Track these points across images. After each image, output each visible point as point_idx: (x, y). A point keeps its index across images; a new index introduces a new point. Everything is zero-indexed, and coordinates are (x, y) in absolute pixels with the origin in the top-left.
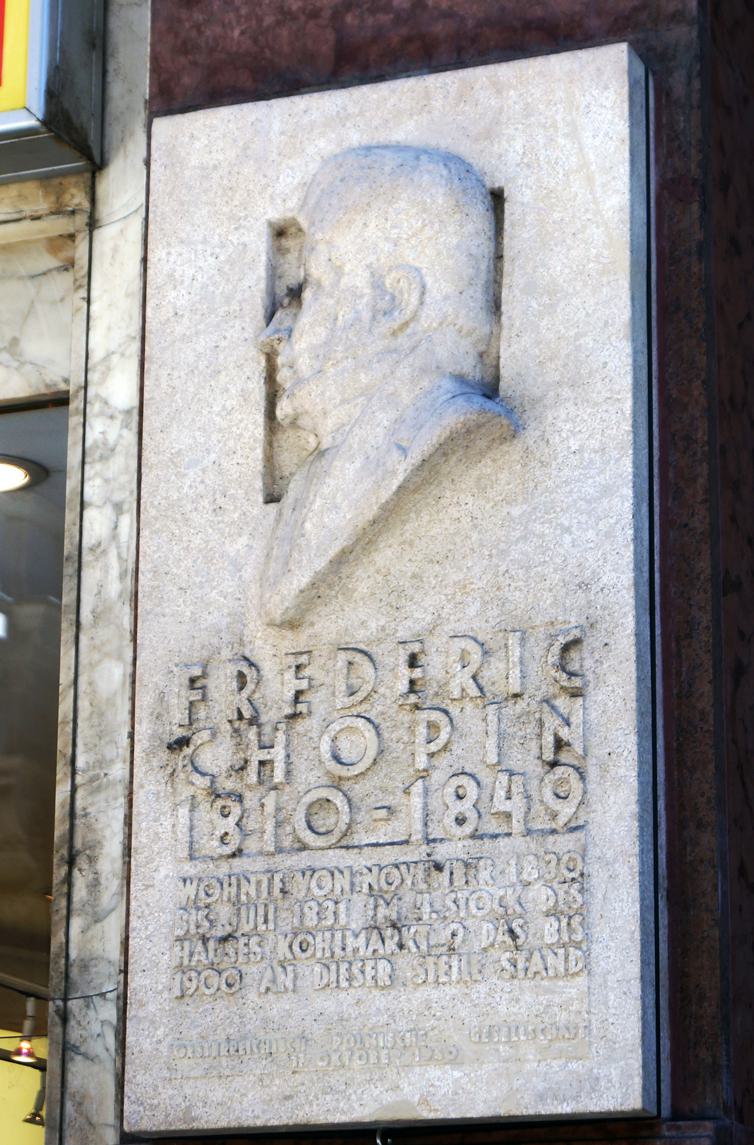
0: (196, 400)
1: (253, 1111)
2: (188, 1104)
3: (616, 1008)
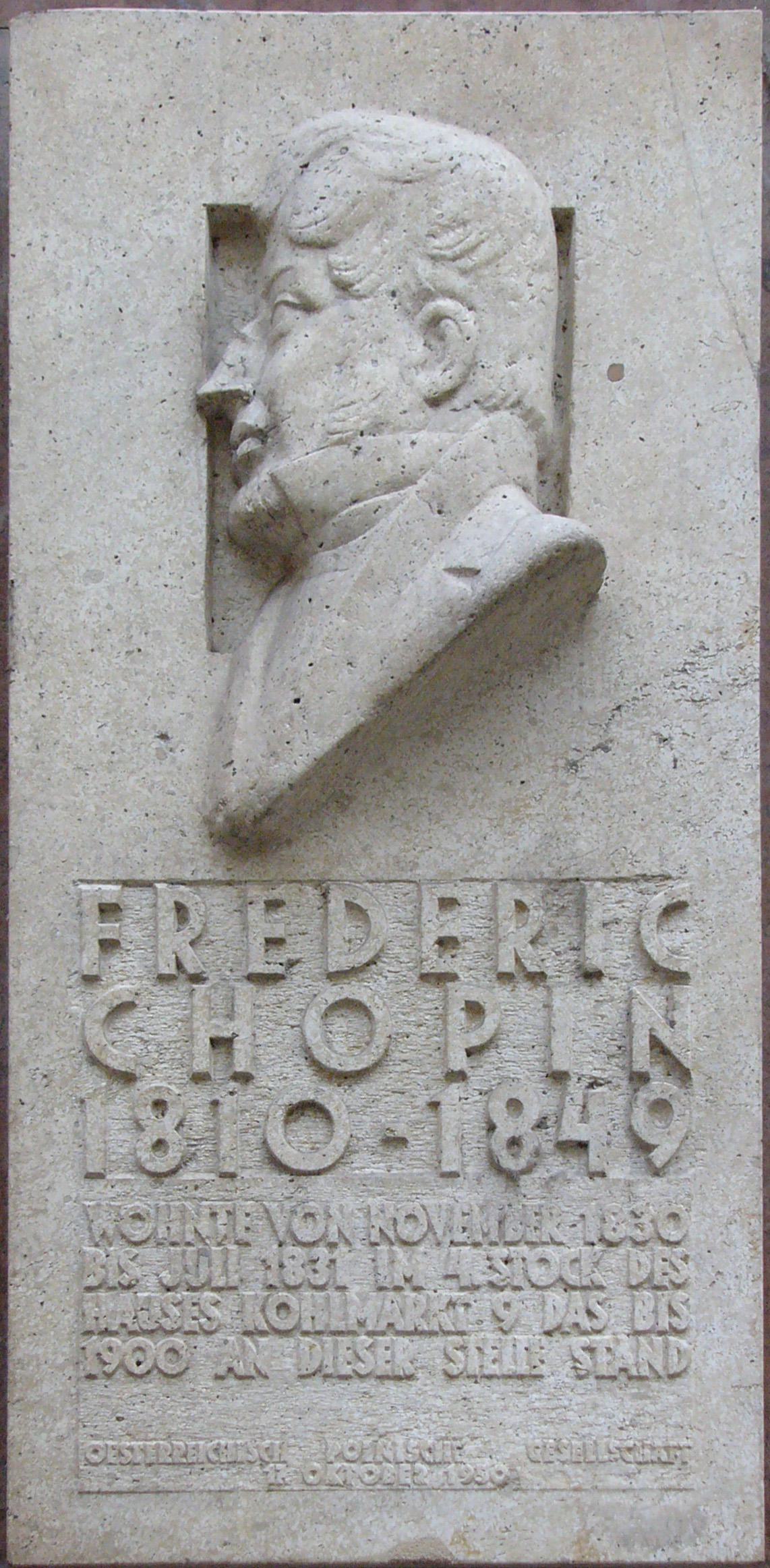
0: (95, 478)
1: (208, 1543)
2: (108, 1529)
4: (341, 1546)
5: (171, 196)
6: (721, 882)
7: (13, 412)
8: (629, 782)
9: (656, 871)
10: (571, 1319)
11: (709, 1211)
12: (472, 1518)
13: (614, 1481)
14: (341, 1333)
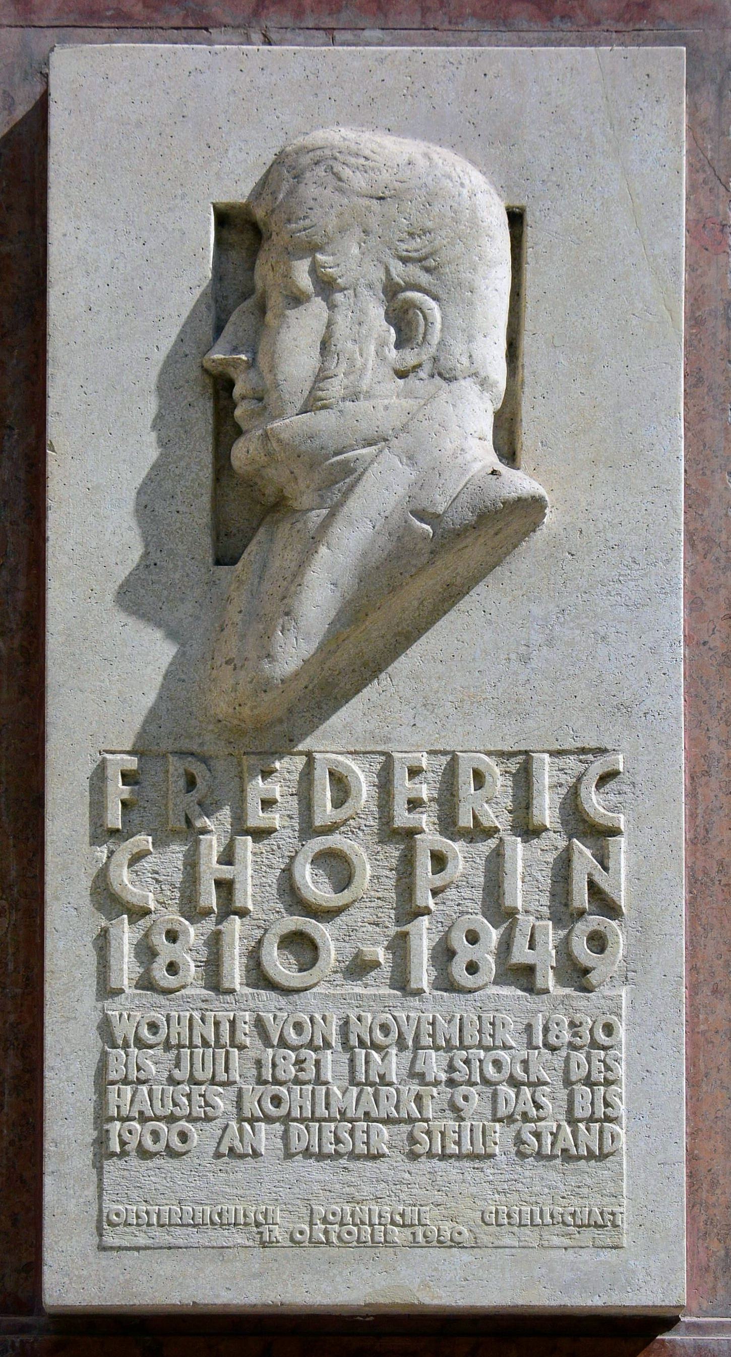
1: (212, 1289)
2: (128, 1277)
3: (656, 1194)
4: (325, 1292)
5: (183, 196)
6: (650, 753)
7: (50, 370)
8: (571, 672)
9: (593, 744)
10: (521, 1108)
11: (639, 1021)
12: (436, 1269)
13: (556, 1241)
14: (325, 1120)
